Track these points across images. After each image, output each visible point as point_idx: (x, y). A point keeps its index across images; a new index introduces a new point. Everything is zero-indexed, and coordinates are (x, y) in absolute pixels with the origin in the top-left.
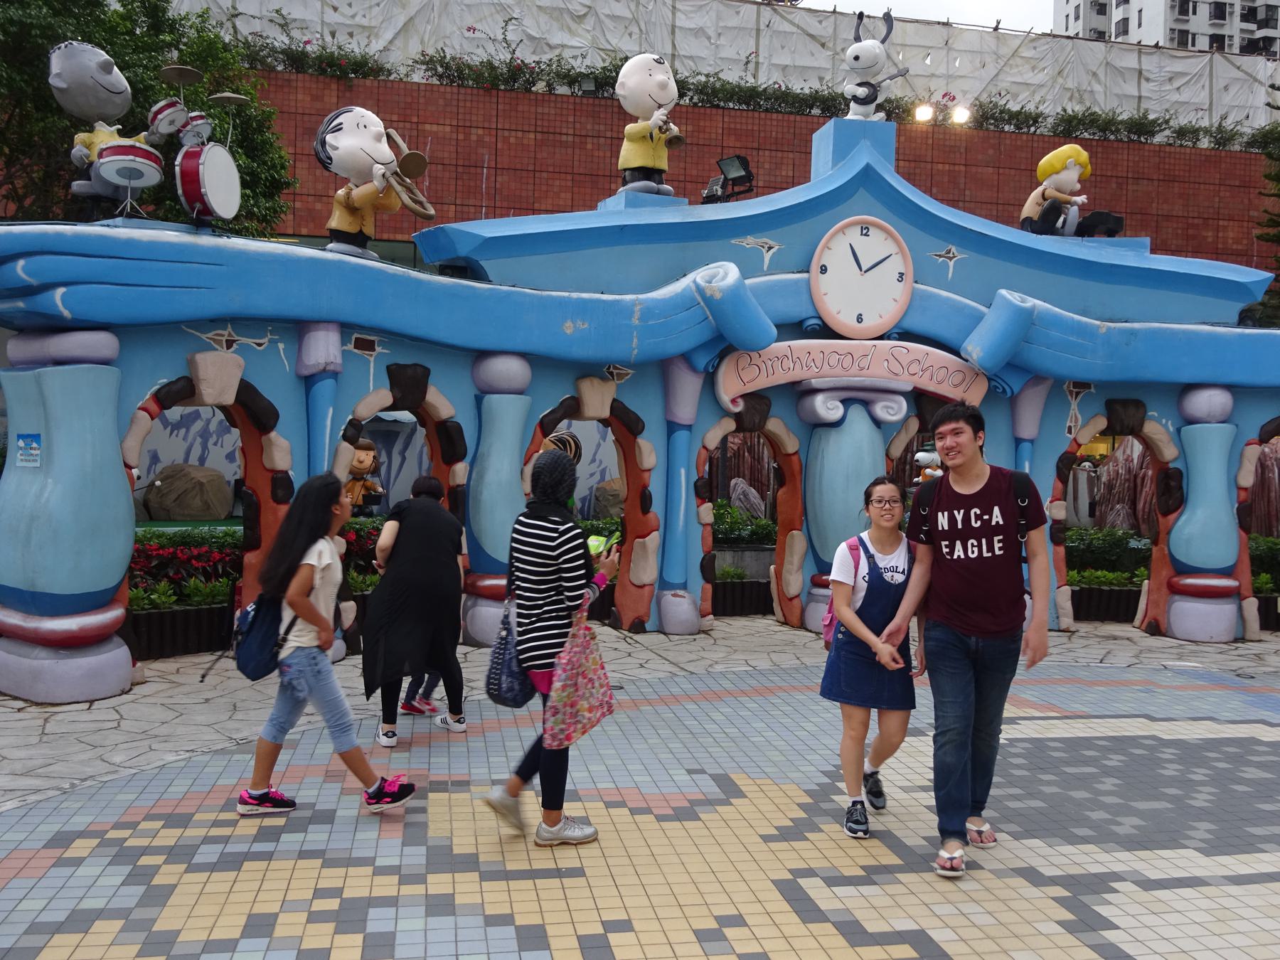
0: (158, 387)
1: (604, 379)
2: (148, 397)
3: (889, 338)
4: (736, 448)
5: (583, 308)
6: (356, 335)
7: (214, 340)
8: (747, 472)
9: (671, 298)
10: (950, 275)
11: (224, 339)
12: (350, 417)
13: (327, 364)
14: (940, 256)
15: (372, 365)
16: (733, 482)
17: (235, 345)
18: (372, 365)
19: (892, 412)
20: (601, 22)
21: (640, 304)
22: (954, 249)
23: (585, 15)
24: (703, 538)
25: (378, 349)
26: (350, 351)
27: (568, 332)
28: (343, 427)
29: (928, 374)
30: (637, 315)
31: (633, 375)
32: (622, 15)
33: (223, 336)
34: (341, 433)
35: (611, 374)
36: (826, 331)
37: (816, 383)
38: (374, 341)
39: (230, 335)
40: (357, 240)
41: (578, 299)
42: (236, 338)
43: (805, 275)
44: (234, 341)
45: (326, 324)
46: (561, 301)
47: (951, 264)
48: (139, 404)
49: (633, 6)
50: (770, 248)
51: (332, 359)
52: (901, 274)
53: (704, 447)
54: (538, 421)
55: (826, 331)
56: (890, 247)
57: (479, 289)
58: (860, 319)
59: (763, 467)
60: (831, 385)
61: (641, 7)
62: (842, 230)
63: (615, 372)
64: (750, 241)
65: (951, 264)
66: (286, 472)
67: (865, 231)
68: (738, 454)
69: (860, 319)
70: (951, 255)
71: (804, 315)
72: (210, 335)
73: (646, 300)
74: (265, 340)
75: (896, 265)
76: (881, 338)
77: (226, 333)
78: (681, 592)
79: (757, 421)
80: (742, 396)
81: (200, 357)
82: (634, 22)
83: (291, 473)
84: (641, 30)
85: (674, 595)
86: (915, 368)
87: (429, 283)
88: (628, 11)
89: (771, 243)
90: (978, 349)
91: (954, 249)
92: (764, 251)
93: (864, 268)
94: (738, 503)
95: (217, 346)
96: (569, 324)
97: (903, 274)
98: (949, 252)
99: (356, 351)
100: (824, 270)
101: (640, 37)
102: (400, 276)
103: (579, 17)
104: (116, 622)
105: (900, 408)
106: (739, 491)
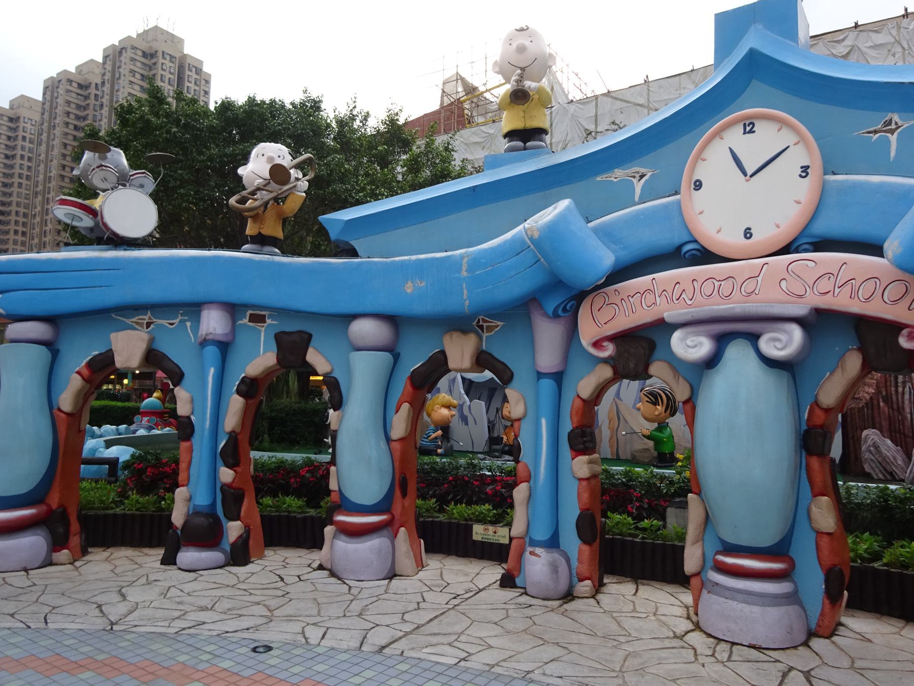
0: (91, 357)
1: (464, 331)
2: (83, 364)
3: (797, 251)
4: (868, 398)
5: (420, 268)
6: (250, 312)
7: (137, 323)
8: (885, 424)
9: (499, 246)
10: (893, 153)
11: (145, 322)
12: (243, 375)
13: (207, 334)
14: (875, 132)
15: (263, 334)
16: (865, 433)
17: (152, 326)
18: (263, 334)
19: (779, 345)
20: (863, 54)
21: (467, 256)
22: (896, 118)
23: (848, 53)
24: (579, 494)
25: (269, 321)
26: (245, 325)
27: (409, 291)
28: (237, 383)
29: (848, 288)
30: (464, 268)
31: (503, 326)
32: (883, 42)
33: (144, 319)
34: (235, 388)
35: (481, 327)
36: (706, 256)
37: (670, 316)
38: (264, 316)
39: (150, 318)
40: (262, 240)
41: (416, 260)
42: (155, 320)
43: (677, 197)
44: (152, 323)
45: (209, 305)
46: (402, 264)
47: (893, 138)
48: (76, 370)
49: (894, 32)
50: (642, 177)
51: (211, 330)
52: (805, 169)
53: (578, 396)
54: (409, 374)
55: (706, 256)
56: (786, 138)
57: (335, 263)
58: (748, 234)
59: (904, 418)
60: (688, 318)
61: (902, 30)
62: (718, 134)
63: (485, 325)
64: (618, 174)
65: (893, 138)
66: (189, 418)
67: (749, 128)
68: (871, 404)
69: (748, 234)
70: (893, 126)
71: (677, 241)
72: (134, 320)
73: (472, 253)
74: (176, 321)
75: (797, 157)
76: (785, 250)
77: (146, 318)
78: (538, 551)
79: (632, 366)
80: (612, 338)
81: (113, 336)
82: (896, 44)
83: (193, 418)
84: (903, 48)
85: (532, 553)
86: (825, 285)
87: (290, 264)
88: (890, 37)
89: (642, 170)
90: (896, 243)
91: (896, 118)
92: (635, 181)
93: (749, 173)
94: (867, 455)
95: (137, 327)
96: (410, 284)
97: (808, 167)
98: (889, 122)
99: (250, 324)
100: (698, 185)
101: (904, 54)
102: (265, 262)
103: (843, 57)
104: (31, 517)
105: (790, 339)
106: (870, 442)
